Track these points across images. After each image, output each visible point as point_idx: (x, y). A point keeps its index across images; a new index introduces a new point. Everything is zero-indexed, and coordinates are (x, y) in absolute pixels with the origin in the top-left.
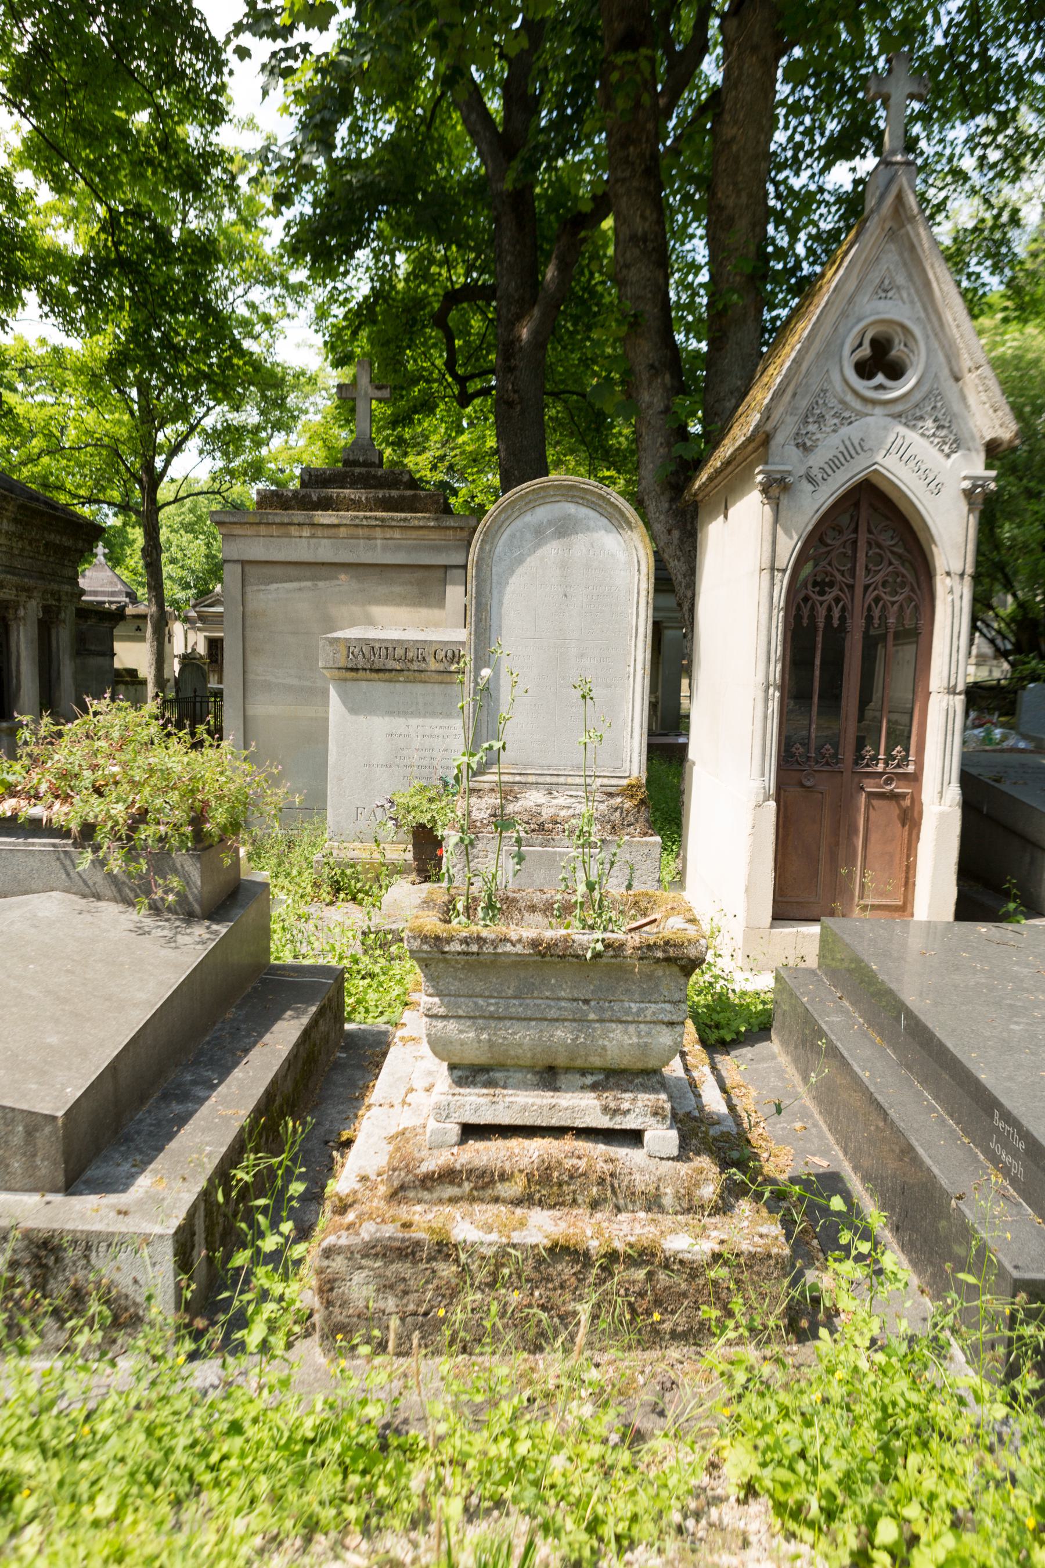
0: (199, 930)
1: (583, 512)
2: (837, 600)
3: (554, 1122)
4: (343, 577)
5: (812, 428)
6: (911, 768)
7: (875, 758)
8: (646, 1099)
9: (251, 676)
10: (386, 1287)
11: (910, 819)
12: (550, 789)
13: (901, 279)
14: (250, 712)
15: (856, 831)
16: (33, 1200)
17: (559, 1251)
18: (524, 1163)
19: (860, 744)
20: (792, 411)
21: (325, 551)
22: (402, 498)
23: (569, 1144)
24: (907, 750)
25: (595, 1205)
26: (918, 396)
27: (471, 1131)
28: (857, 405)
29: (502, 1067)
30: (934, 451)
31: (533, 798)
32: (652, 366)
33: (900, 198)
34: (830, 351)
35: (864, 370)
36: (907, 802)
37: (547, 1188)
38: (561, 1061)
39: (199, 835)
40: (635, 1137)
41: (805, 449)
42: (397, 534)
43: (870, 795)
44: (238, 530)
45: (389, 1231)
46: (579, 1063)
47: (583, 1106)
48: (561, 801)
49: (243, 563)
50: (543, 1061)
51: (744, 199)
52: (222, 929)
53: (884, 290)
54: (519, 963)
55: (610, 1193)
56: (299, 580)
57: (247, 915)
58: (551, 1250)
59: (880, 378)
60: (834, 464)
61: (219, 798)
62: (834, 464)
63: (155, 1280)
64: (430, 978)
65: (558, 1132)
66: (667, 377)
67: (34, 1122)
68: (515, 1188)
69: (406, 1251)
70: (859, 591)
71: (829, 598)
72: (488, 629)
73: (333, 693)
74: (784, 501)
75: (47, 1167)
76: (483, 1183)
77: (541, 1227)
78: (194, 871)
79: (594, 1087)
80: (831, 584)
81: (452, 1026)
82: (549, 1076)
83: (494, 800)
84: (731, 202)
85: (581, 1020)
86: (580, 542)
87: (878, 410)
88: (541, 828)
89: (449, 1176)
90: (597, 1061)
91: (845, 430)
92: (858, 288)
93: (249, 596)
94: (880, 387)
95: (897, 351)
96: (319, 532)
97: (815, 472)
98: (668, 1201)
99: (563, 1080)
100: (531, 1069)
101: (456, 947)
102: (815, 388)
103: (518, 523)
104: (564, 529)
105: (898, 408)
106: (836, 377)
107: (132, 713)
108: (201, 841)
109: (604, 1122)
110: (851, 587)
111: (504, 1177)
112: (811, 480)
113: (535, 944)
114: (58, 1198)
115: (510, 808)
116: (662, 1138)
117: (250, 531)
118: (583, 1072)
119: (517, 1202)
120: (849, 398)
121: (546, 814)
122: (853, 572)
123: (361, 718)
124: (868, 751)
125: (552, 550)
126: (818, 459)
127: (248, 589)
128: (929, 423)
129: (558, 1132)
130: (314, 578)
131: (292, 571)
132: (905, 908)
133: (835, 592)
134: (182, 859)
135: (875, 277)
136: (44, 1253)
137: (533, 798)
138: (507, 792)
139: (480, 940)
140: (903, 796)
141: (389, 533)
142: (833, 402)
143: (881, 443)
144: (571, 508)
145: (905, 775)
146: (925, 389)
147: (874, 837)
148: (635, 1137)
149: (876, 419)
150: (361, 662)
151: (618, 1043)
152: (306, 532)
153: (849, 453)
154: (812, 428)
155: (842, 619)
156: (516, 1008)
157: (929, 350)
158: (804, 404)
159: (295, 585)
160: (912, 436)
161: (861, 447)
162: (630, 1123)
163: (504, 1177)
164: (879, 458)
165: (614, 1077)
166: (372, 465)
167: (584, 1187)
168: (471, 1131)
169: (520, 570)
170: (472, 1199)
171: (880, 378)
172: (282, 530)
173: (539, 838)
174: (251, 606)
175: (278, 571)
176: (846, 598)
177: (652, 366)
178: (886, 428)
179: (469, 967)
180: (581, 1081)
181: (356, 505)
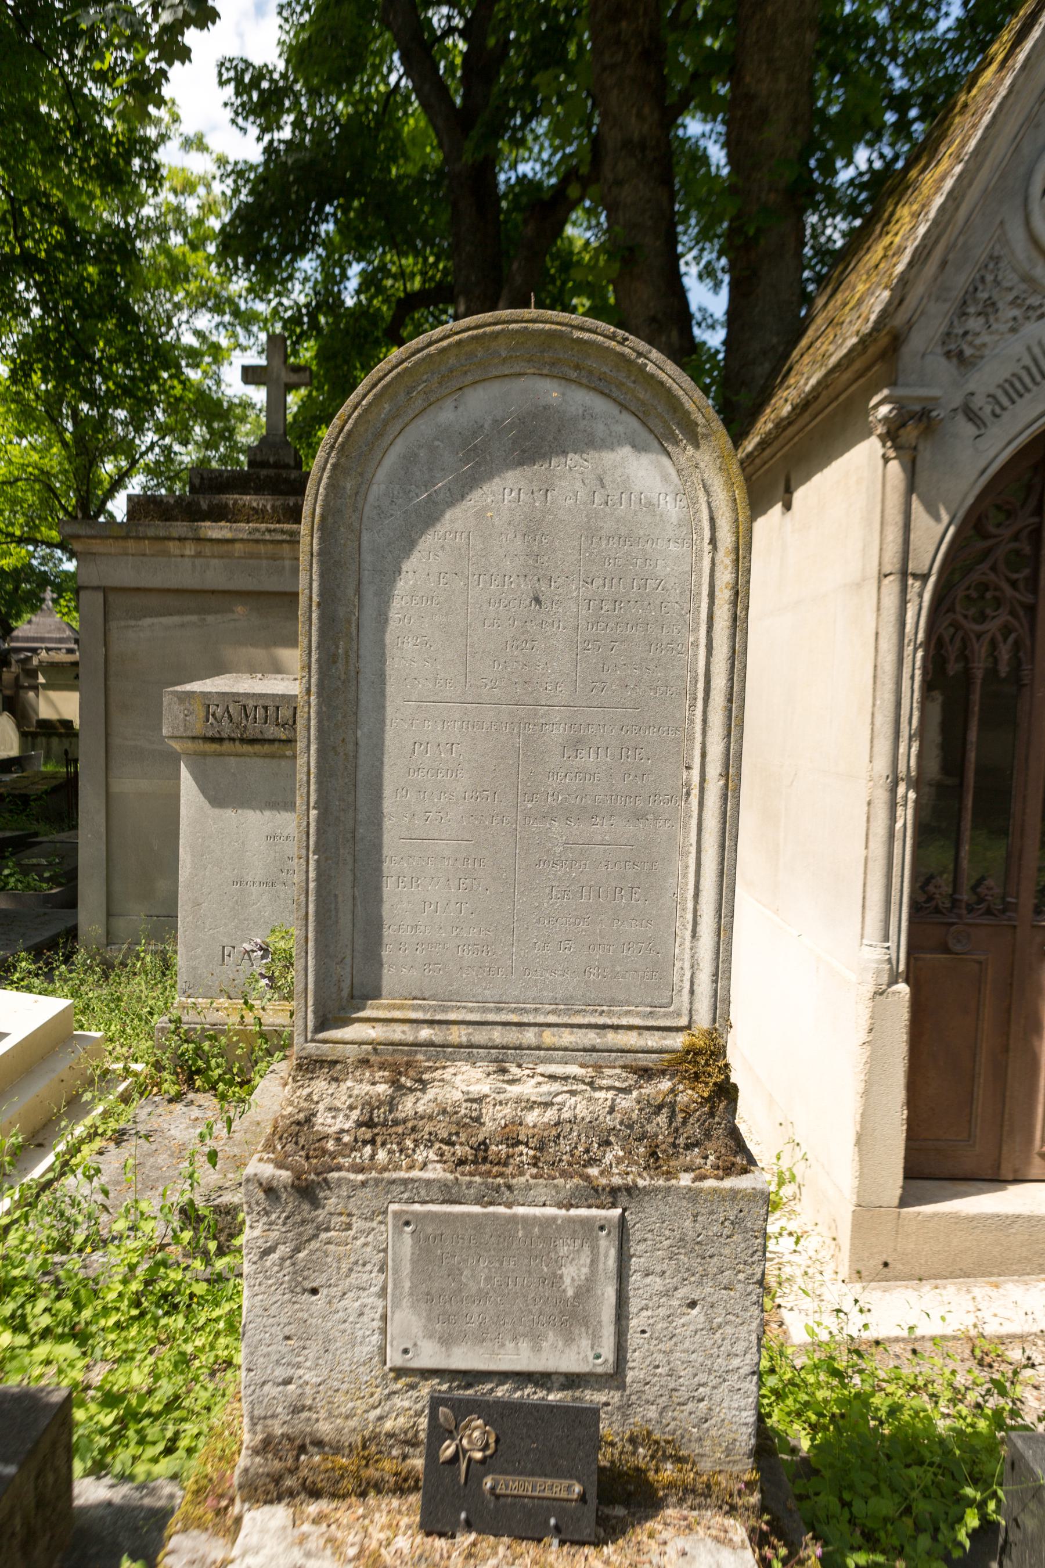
1: (581, 400)
2: (1007, 630)
4: (240, 609)
5: (974, 324)
9: (116, 741)
12: (501, 1060)
14: (116, 788)
21: (215, 575)
31: (464, 1081)
32: (653, 319)
41: (960, 359)
48: (528, 1089)
49: (105, 590)
56: (180, 612)
71: (992, 627)
73: (185, 773)
74: (926, 454)
80: (998, 602)
86: (572, 475)
96: (207, 549)
103: (422, 429)
104: (534, 442)
112: (971, 415)
115: (408, 1106)
121: (494, 1118)
123: (229, 813)
125: (503, 494)
126: (985, 380)
127: (113, 624)
137: (464, 1081)
138: (404, 1066)
142: (1010, 278)
150: (226, 728)
152: (190, 549)
154: (974, 324)
155: (1016, 664)
158: (961, 281)
159: (176, 619)
166: (286, 466)
169: (429, 541)
181: (259, 515)
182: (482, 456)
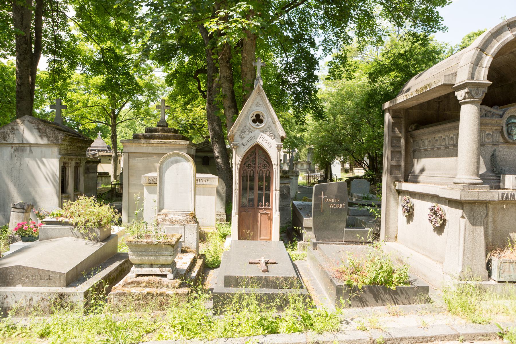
0: (99, 244)
1: (181, 158)
2: (252, 170)
3: (152, 273)
4: (155, 156)
5: (243, 134)
6: (270, 207)
7: (262, 205)
8: (168, 269)
9: (130, 182)
10: (120, 301)
11: (270, 219)
12: (175, 214)
13: (261, 103)
14: (130, 191)
15: (258, 221)
16: (60, 288)
17: (149, 294)
18: (146, 280)
19: (258, 203)
20: (239, 130)
21: (150, 150)
22: (171, 136)
23: (154, 277)
24: (269, 203)
25: (157, 287)
26: (266, 127)
27: (139, 275)
28: (253, 129)
29: (143, 264)
30: (270, 138)
31: (171, 216)
32: (229, 107)
33: (259, 87)
34: (246, 118)
35: (254, 121)
36: (269, 215)
37: (149, 284)
38: (153, 263)
39: (100, 225)
40: (165, 276)
41: (242, 138)
42: (169, 146)
43: (261, 214)
44: (127, 145)
45: (121, 291)
46: (156, 263)
47: (157, 271)
48: (177, 217)
49: (128, 153)
50: (150, 263)
51: (249, 70)
52: (104, 244)
53: (258, 105)
54: (144, 245)
55: (160, 285)
56: (143, 157)
57: (111, 241)
58: (147, 293)
59: (258, 123)
60: (248, 141)
61: (104, 217)
62: (248, 141)
63: (80, 301)
64: (130, 248)
65: (152, 275)
66: (233, 109)
67: (61, 274)
68: (144, 285)
69: (123, 294)
70: (257, 168)
71: (250, 169)
72: (162, 182)
73: (145, 189)
74: (237, 149)
75: (63, 282)
76: (139, 283)
77: (147, 290)
78: (99, 232)
79: (159, 267)
80: (251, 166)
81: (134, 256)
82: (151, 266)
83: (163, 217)
84: (246, 70)
85: (155, 256)
86: (180, 164)
87: (257, 130)
88: (173, 222)
89: (132, 283)
90: (159, 263)
91: (250, 134)
92: (252, 104)
93: (130, 161)
94: (258, 125)
95: (261, 118)
96: (149, 145)
97: (244, 143)
98: (170, 286)
99: (154, 266)
100: (148, 264)
101: (134, 243)
102: (244, 125)
103: (168, 161)
104: (177, 162)
105: (262, 129)
106: (248, 123)
107: (88, 200)
108: (100, 225)
109: (160, 273)
110: (255, 167)
111: (142, 283)
112: (243, 145)
113: (146, 242)
114: (65, 288)
115: (166, 218)
116: (170, 276)
117: (130, 145)
118: (157, 265)
119: (144, 287)
120: (251, 127)
121: (174, 219)
122: (255, 164)
123: (152, 195)
124: (260, 204)
125: (175, 166)
126: (245, 140)
127: (130, 159)
128: (268, 132)
129: (152, 275)
130: (147, 157)
131: (141, 155)
132: (270, 239)
133: (252, 168)
134: (96, 230)
135: (256, 102)
136: (62, 296)
137: (171, 216)
138: (166, 215)
139: (137, 241)
140: (268, 214)
141: (167, 145)
142: (247, 128)
143: (258, 136)
144: (178, 158)
145: (269, 209)
146: (267, 125)
147: (262, 223)
148: (165, 276)
149: (257, 131)
150: (152, 182)
151: (162, 260)
152: (145, 145)
153: (251, 139)
154: (243, 134)
155: (254, 174)
156: (144, 253)
157: (268, 118)
158: (241, 129)
159: (142, 158)
160: (265, 135)
161: (254, 138)
162: (164, 273)
163: (142, 283)
164: (258, 140)
165: (162, 266)
166: (164, 126)
167: (155, 284)
168: (139, 275)
169: (168, 170)
170: (136, 287)
171: (258, 123)
172: (139, 144)
173: (172, 224)
174: (130, 164)
175: (138, 155)
176: (254, 170)
177: (229, 107)
178: (259, 134)
179: (136, 246)
180: (156, 266)
181: (160, 138)
182: (172, 163)
